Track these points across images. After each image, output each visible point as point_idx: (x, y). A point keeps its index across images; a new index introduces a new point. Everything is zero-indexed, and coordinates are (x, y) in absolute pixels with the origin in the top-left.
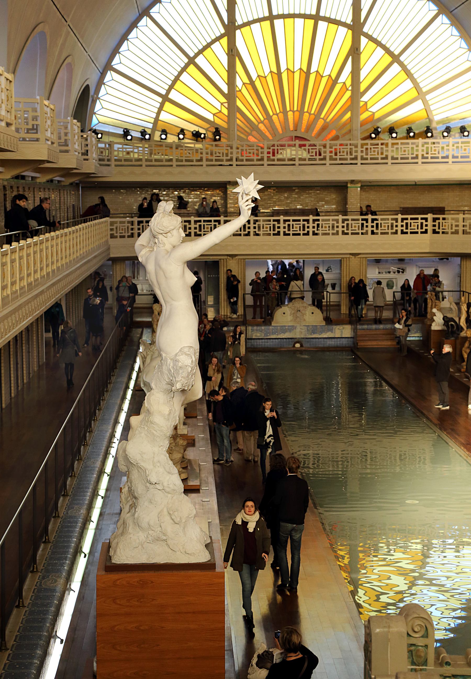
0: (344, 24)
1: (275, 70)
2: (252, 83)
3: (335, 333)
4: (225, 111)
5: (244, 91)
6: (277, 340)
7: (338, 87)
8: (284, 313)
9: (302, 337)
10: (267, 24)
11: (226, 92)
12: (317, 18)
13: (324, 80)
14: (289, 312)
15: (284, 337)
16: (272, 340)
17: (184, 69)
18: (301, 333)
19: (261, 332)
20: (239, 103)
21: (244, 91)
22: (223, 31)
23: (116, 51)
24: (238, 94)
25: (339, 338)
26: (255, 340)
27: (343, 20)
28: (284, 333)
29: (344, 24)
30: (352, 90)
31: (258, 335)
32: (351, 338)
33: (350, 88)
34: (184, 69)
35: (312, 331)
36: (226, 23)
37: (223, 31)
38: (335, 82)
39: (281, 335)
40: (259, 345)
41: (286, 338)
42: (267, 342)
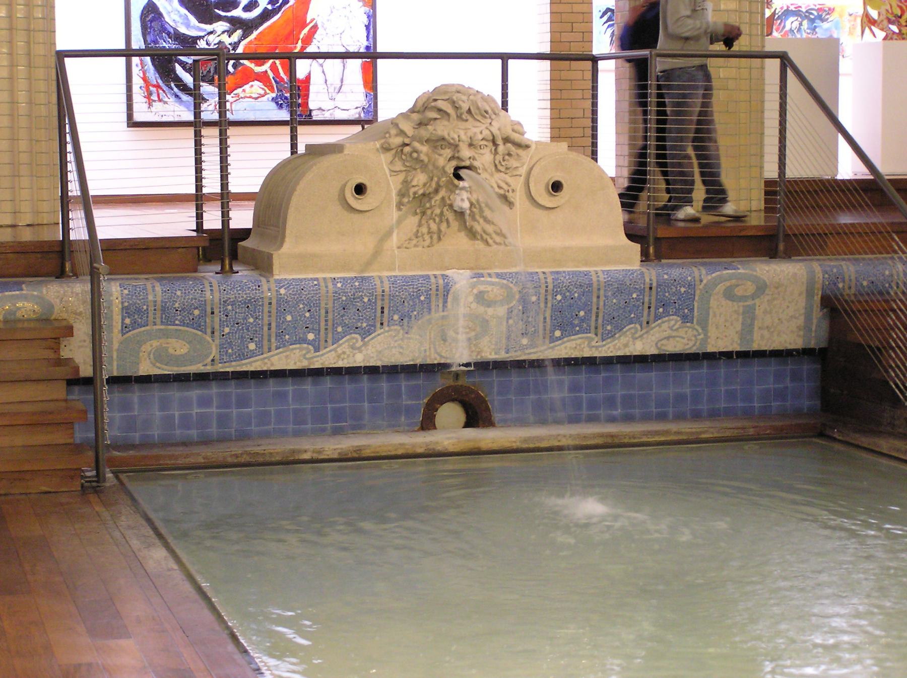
3: (704, 323)
6: (308, 386)
8: (360, 189)
9: (490, 355)
14: (394, 184)
15: (359, 360)
16: (272, 386)
18: (481, 325)
19: (197, 324)
25: (728, 355)
26: (156, 393)
28: (366, 333)
31: (179, 347)
32: (806, 352)
35: (558, 310)
39: (344, 345)
40: (186, 422)
41: (372, 371)
42: (243, 402)
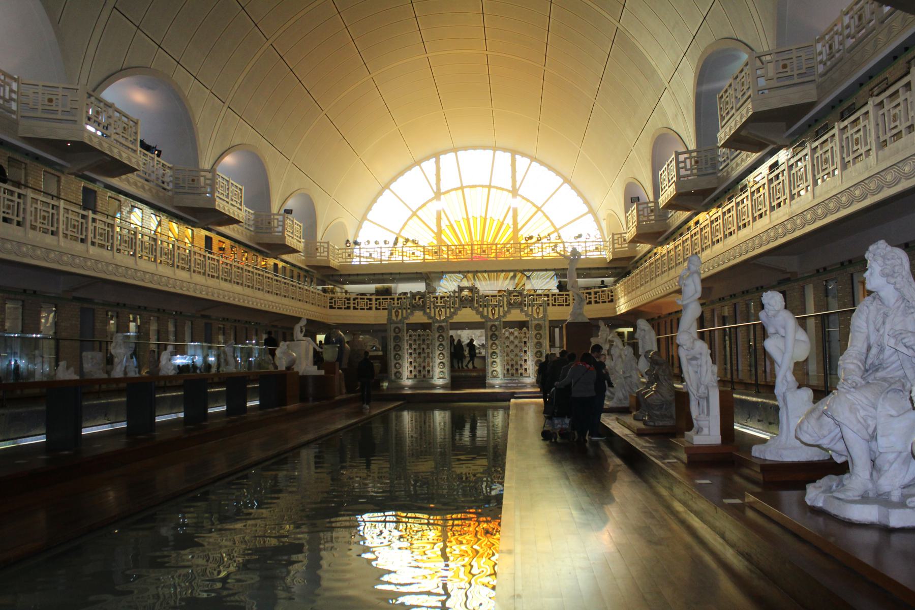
0: (507, 190)
1: (465, 217)
2: (451, 225)
4: (435, 242)
5: (446, 229)
7: (504, 226)
10: (460, 191)
11: (436, 231)
12: (490, 187)
13: (496, 222)
17: (410, 218)
20: (443, 237)
21: (446, 229)
22: (434, 196)
23: (369, 208)
24: (443, 231)
27: (505, 188)
29: (507, 190)
30: (513, 228)
33: (512, 226)
34: (410, 218)
36: (435, 190)
37: (434, 196)
38: (502, 224)
